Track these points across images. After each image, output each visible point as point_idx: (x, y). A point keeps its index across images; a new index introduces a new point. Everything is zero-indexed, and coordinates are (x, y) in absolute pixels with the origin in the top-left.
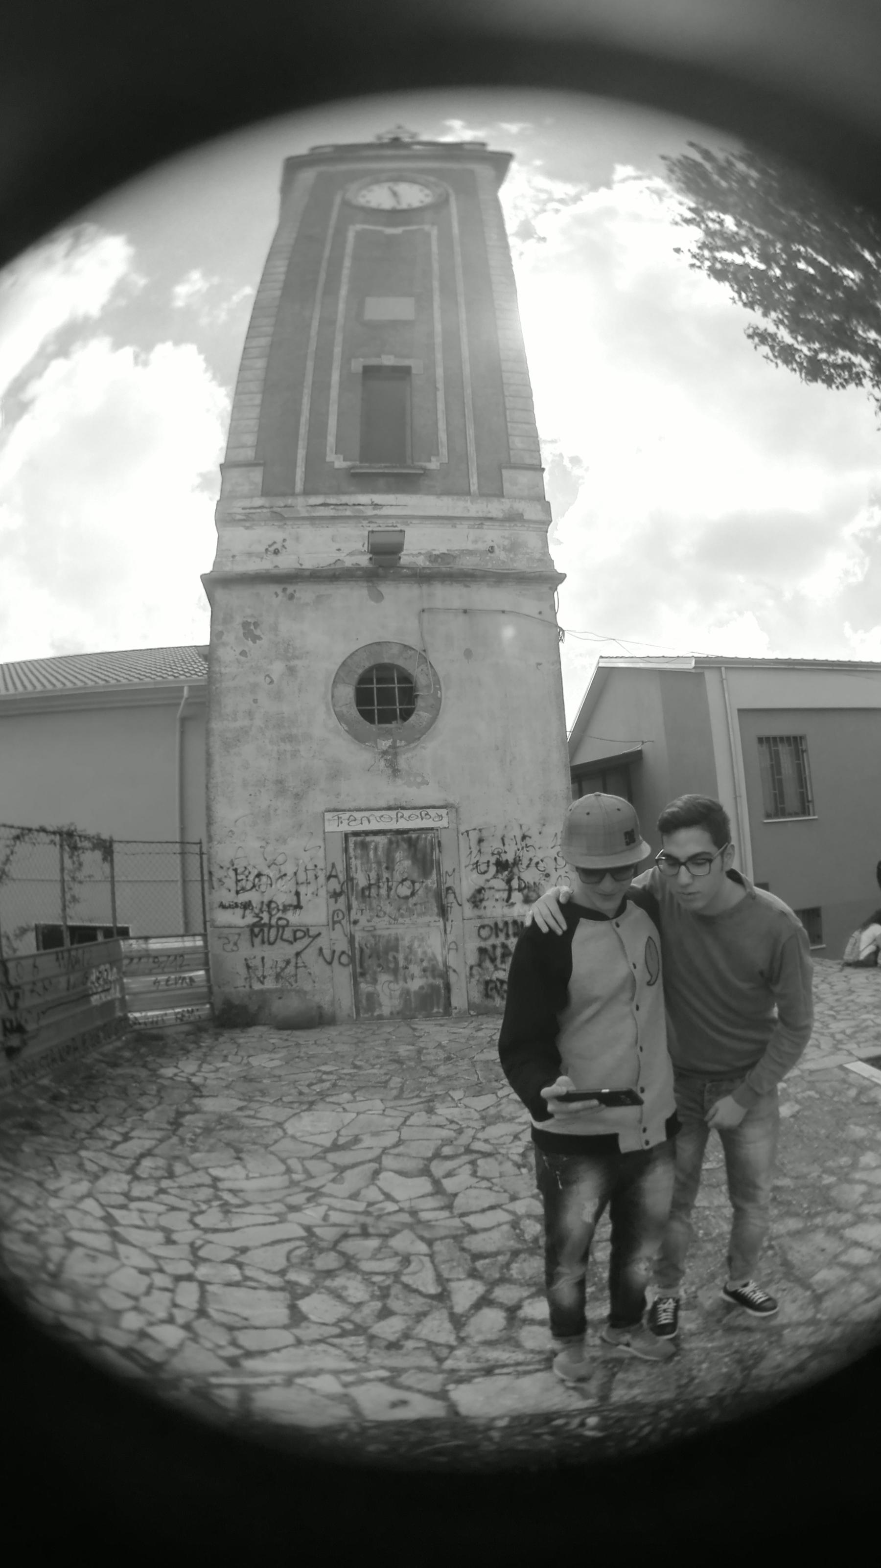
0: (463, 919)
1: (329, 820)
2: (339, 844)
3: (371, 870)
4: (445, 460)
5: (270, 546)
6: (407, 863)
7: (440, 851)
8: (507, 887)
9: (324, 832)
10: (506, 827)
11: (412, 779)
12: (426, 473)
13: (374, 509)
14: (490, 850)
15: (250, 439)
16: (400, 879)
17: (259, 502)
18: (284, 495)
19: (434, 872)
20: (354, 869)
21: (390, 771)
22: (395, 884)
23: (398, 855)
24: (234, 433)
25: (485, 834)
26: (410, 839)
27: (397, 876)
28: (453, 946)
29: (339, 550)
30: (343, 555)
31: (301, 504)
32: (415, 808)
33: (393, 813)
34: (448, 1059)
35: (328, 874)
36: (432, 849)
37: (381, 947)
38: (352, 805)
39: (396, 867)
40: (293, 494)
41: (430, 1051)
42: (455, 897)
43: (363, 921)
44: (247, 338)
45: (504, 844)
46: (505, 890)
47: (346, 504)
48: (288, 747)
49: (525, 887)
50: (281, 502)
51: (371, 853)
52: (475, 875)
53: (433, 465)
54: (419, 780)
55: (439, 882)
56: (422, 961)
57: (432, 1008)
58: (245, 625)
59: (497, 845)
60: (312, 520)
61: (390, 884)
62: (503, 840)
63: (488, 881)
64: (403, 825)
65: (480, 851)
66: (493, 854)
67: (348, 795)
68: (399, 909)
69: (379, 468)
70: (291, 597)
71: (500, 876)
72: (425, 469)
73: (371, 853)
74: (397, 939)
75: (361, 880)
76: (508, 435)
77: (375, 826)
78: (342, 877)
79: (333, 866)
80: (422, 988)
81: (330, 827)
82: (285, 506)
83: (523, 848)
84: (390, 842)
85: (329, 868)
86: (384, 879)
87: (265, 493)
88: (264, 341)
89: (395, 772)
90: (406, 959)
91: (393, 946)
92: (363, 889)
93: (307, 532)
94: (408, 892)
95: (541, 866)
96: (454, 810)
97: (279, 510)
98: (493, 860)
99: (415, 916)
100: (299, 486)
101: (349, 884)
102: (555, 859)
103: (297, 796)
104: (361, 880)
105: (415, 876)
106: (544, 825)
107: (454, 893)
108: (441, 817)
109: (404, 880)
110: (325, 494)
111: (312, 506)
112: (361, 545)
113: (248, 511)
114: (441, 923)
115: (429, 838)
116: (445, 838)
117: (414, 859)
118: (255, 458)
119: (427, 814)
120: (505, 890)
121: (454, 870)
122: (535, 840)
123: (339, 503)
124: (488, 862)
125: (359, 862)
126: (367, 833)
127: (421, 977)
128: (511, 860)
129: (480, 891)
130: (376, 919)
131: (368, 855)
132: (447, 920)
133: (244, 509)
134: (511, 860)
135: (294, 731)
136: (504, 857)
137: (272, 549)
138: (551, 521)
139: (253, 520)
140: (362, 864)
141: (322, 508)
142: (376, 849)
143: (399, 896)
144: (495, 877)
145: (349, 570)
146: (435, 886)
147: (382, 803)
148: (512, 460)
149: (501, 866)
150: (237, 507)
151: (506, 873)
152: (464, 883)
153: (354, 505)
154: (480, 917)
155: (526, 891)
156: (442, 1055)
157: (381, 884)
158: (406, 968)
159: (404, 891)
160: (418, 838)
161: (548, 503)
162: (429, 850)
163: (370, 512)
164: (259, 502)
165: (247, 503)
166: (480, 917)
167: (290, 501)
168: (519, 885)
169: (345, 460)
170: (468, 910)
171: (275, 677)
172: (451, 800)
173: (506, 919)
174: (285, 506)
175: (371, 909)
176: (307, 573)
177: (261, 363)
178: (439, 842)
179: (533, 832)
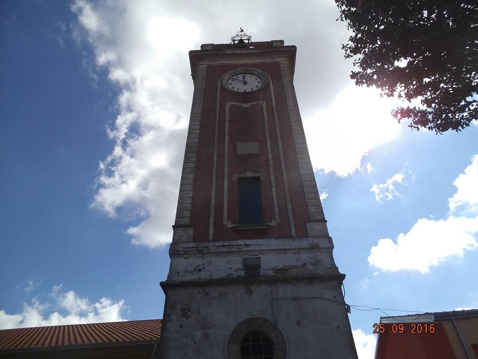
5: (197, 267)
13: (246, 247)
17: (192, 245)
29: (230, 268)
40: (208, 241)
47: (233, 245)
58: (183, 310)
60: (218, 254)
70: (207, 294)
72: (269, 226)
87: (194, 241)
88: (192, 165)
97: (201, 249)
100: (211, 237)
110: (223, 240)
112: (240, 266)
113: (186, 249)
137: (198, 269)
138: (333, 247)
145: (235, 278)
150: (181, 247)
153: (237, 245)
161: (331, 237)
163: (245, 249)
164: (192, 245)
165: (185, 245)
167: (206, 244)
171: (197, 340)
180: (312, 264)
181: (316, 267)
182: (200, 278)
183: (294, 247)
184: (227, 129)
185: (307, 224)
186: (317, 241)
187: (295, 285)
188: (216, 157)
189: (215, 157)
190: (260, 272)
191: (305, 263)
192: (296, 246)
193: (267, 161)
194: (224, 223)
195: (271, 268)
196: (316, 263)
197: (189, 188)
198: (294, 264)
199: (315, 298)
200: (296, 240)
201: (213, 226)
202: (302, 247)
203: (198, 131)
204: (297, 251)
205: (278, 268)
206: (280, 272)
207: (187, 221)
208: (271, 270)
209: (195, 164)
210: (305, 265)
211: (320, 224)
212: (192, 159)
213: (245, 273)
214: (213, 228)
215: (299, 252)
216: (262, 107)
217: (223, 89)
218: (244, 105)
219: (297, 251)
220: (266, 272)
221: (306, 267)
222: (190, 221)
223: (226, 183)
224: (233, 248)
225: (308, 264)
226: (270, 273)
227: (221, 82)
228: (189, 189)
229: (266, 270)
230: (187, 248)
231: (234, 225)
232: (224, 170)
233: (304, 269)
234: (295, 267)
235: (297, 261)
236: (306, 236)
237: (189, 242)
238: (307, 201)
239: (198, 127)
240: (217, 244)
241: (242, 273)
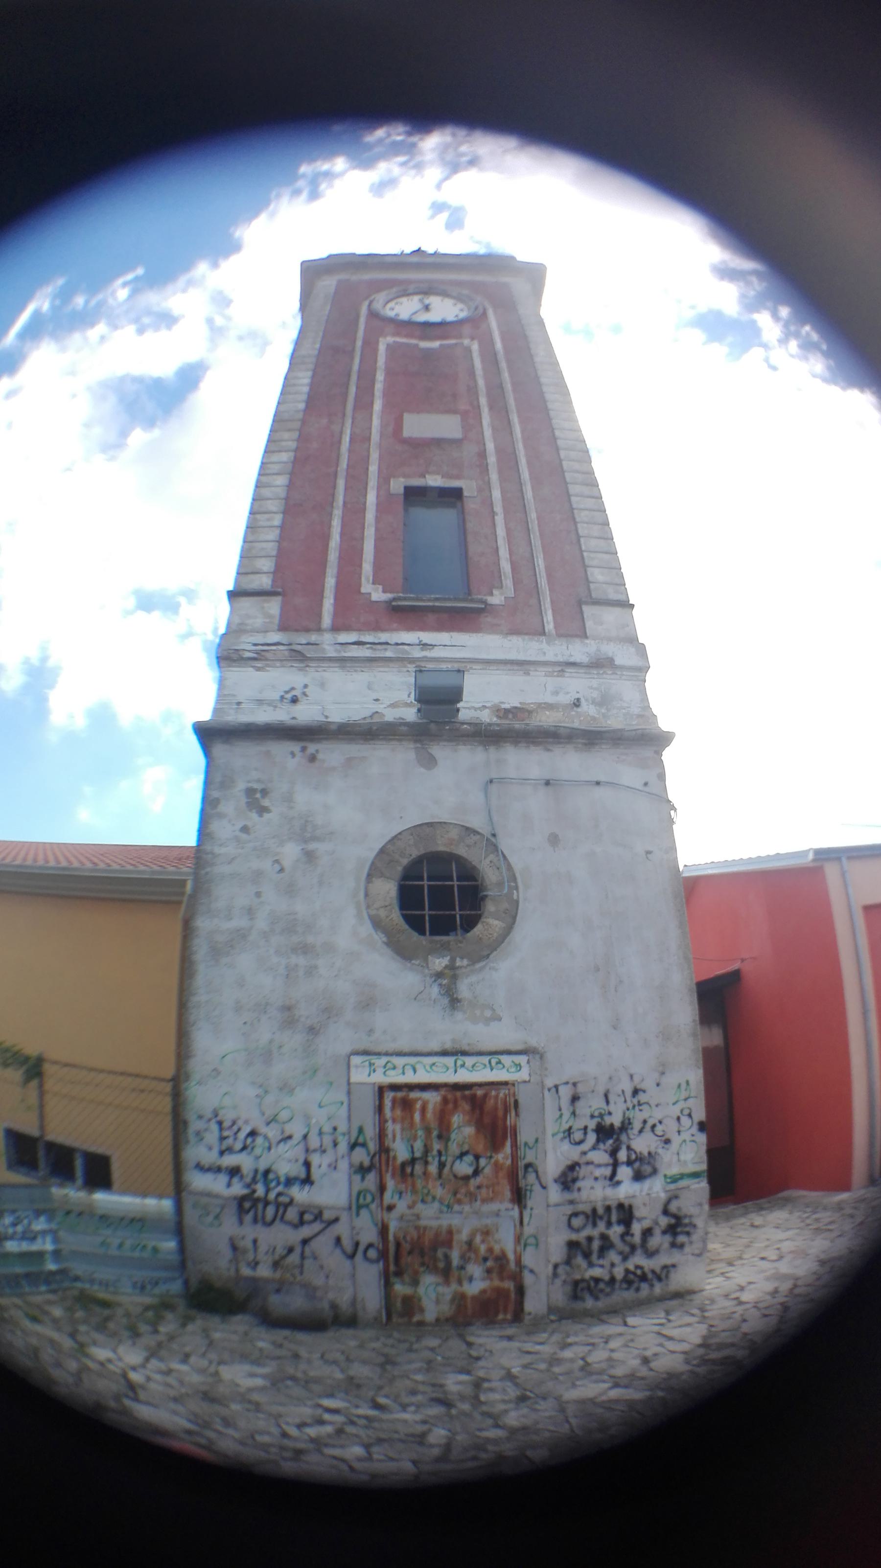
0: (548, 1206)
1: (357, 1067)
2: (368, 1102)
3: (415, 1138)
4: (511, 594)
6: (469, 1131)
7: (517, 1115)
8: (611, 1161)
9: (349, 1084)
10: (610, 1078)
11: (478, 1012)
12: (486, 609)
13: (422, 650)
14: (588, 1112)
16: (457, 1152)
17: (274, 637)
18: (307, 630)
19: (508, 1144)
20: (390, 1136)
21: (446, 1001)
22: (450, 1159)
23: (457, 1119)
24: (247, 555)
25: (581, 1089)
26: (473, 1097)
27: (454, 1149)
28: (532, 1240)
29: (377, 700)
30: (382, 706)
31: (328, 643)
32: (481, 1054)
33: (449, 1061)
34: (522, 1399)
35: (353, 1141)
36: (506, 1110)
37: (427, 1241)
38: (391, 1047)
39: (453, 1136)
40: (319, 630)
41: (493, 1385)
42: (538, 1177)
43: (402, 1206)
44: (266, 452)
45: (608, 1102)
46: (607, 1165)
47: (387, 643)
48: (301, 961)
49: (636, 1160)
50: (303, 639)
51: (417, 1117)
52: (566, 1146)
53: (496, 599)
54: (488, 1013)
55: (515, 1157)
56: (485, 1259)
57: (497, 1313)
59: (597, 1103)
60: (342, 662)
61: (443, 1158)
62: (606, 1096)
63: (584, 1153)
64: (464, 1076)
65: (574, 1113)
66: (592, 1117)
67: (385, 1032)
68: (455, 1193)
69: (429, 600)
71: (601, 1146)
73: (417, 1117)
74: (450, 1232)
75: (401, 1151)
76: (585, 567)
77: (423, 1077)
78: (372, 1146)
79: (361, 1130)
80: (484, 1292)
81: (359, 1076)
82: (308, 644)
83: (634, 1107)
84: (445, 1101)
85: (354, 1134)
86: (435, 1152)
87: (283, 627)
89: (454, 1002)
90: (463, 1257)
91: (446, 1239)
92: (404, 1165)
93: (335, 677)
94: (469, 1171)
95: (659, 1129)
96: (537, 1057)
97: (299, 648)
98: (592, 1124)
99: (478, 1203)
100: (327, 620)
101: (384, 1157)
103: (312, 1031)
104: (401, 1151)
105: (480, 1148)
106: (663, 1073)
107: (536, 1172)
108: (519, 1067)
109: (462, 1155)
110: (359, 630)
111: (342, 644)
114: (516, 1212)
115: (501, 1095)
116: (524, 1096)
117: (480, 1125)
118: (272, 586)
119: (499, 1062)
120: (607, 1165)
121: (537, 1141)
122: (651, 1095)
123: (376, 641)
124: (586, 1128)
125: (398, 1127)
126: (411, 1087)
127: (483, 1279)
128: (617, 1123)
129: (572, 1167)
130: (420, 1207)
131: (412, 1117)
132: (525, 1207)
133: (255, 645)
134: (617, 1123)
135: (310, 939)
136: (608, 1120)
139: (267, 660)
140: (403, 1129)
142: (424, 1110)
143: (455, 1176)
144: (594, 1148)
146: (509, 1162)
147: (435, 1046)
148: (594, 595)
149: (604, 1132)
150: (246, 644)
151: (611, 1142)
152: (551, 1157)
153: (397, 644)
154: (571, 1202)
155: (637, 1165)
156: (513, 1392)
157: (430, 1159)
158: (462, 1268)
159: (464, 1168)
160: (485, 1096)
162: (500, 1113)
163: (417, 653)
164: (274, 637)
165: (259, 638)
166: (571, 1202)
167: (313, 637)
168: (629, 1157)
169: (384, 591)
170: (555, 1194)
171: (287, 863)
172: (533, 1042)
173: (607, 1203)
174: (308, 644)
175: (414, 1191)
176: (334, 727)
177: (282, 481)
178: (516, 1103)
179: (649, 1084)
180: (594, 702)
181: (603, 711)
182: (294, 718)
183: (550, 657)
184: (379, 387)
185: (584, 608)
186: (609, 649)
187: (548, 750)
188: (348, 439)
189: (346, 439)
190: (458, 710)
191: (578, 700)
192: (556, 655)
193: (482, 455)
194: (363, 590)
195: (488, 705)
196: (605, 701)
197: (274, 506)
198: (550, 699)
199: (598, 783)
200: (556, 642)
201: (332, 597)
202: (572, 660)
203: (306, 389)
204: (560, 668)
205: (507, 706)
206: (510, 716)
207: (265, 582)
208: (487, 711)
209: (292, 454)
210: (577, 704)
211: (617, 611)
212: (284, 444)
214: (332, 601)
215: (563, 671)
216: (468, 350)
217: (373, 315)
218: (424, 344)
219: (560, 668)
220: (477, 714)
221: (579, 710)
222: (274, 581)
223: (371, 498)
224: (386, 650)
225: (583, 702)
226: (486, 717)
227: (369, 305)
228: (274, 509)
229: (476, 709)
231: (388, 596)
232: (367, 469)
233: (573, 713)
234: (550, 707)
235: (556, 693)
236: (583, 635)
237: (266, 632)
238: (585, 554)
239: (307, 381)
240: (344, 637)
241: (410, 714)
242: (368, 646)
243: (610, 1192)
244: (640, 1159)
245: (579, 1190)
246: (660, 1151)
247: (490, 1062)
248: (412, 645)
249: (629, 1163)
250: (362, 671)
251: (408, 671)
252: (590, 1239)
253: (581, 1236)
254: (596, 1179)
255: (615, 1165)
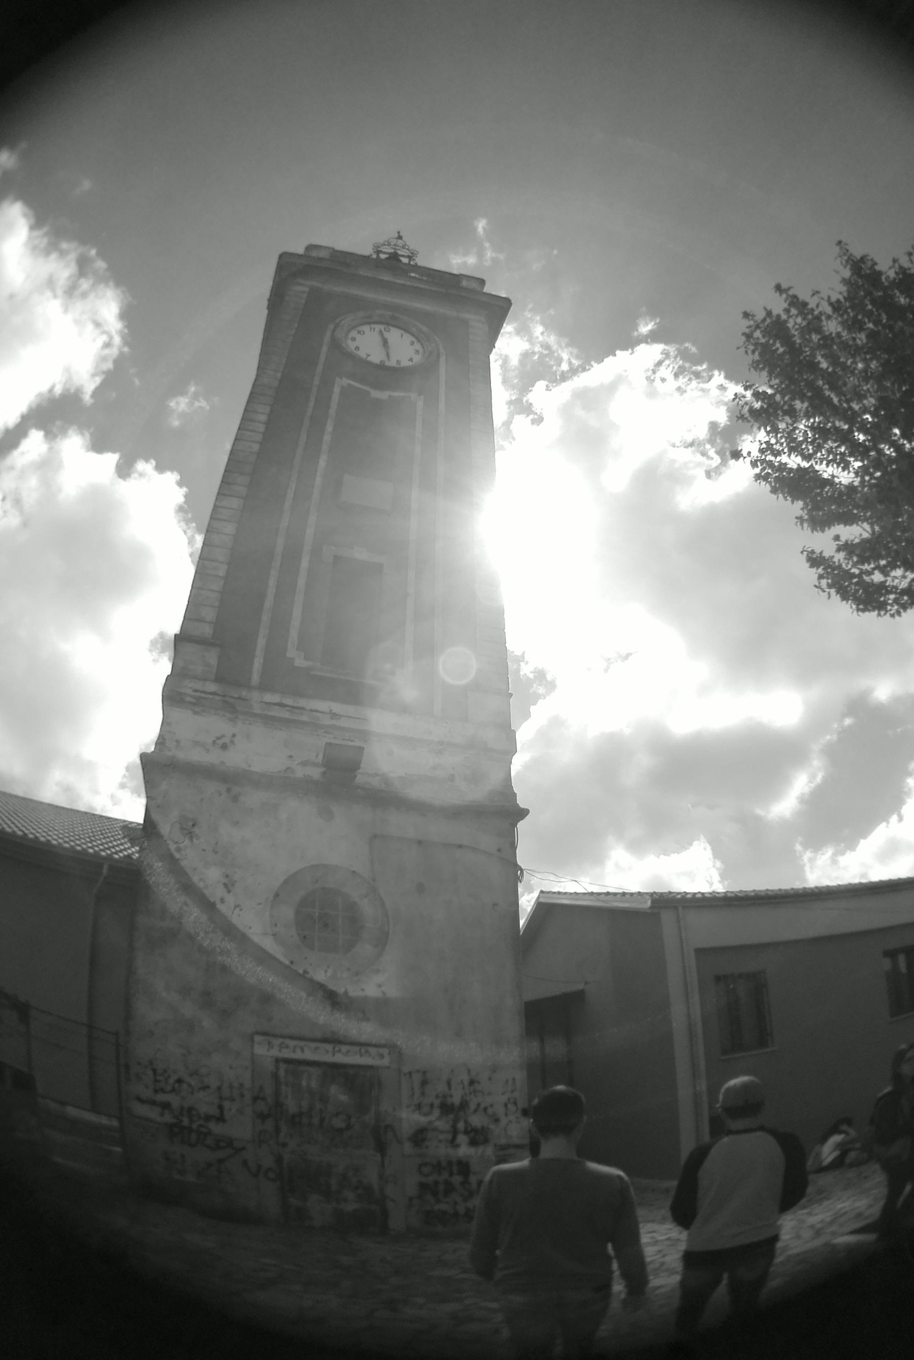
5: (218, 738)
15: (209, 614)
29: (291, 757)
40: (249, 687)
47: (303, 709)
82: (239, 698)
87: (219, 679)
97: (232, 700)
102: (506, 1105)
111: (267, 703)
113: (198, 694)
133: (196, 691)
137: (220, 742)
141: (277, 707)
153: (312, 710)
163: (327, 721)
164: (212, 687)
167: (244, 693)
174: (239, 698)
190: (355, 777)
191: (453, 775)
199: (460, 846)
210: (452, 778)
213: (324, 773)
224: (302, 714)
230: (201, 692)
240: (270, 698)
241: (316, 773)
242: (288, 708)
243: (451, 1151)
244: (475, 1130)
245: (427, 1147)
246: (492, 1127)
247: (360, 1051)
248: (324, 713)
249: (466, 1132)
250: (281, 729)
251: (318, 735)
252: (436, 1183)
253: (431, 1179)
254: (440, 1141)
255: (455, 1132)
